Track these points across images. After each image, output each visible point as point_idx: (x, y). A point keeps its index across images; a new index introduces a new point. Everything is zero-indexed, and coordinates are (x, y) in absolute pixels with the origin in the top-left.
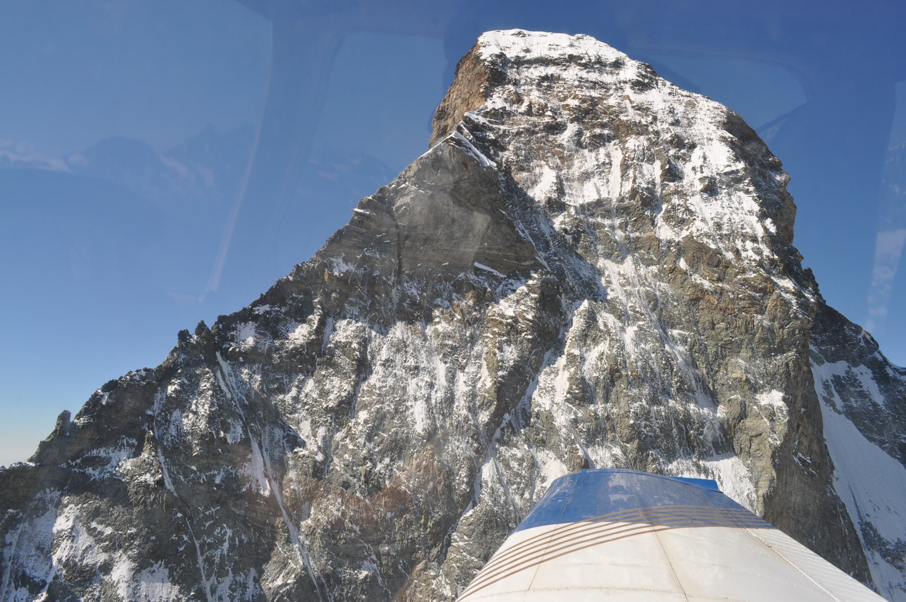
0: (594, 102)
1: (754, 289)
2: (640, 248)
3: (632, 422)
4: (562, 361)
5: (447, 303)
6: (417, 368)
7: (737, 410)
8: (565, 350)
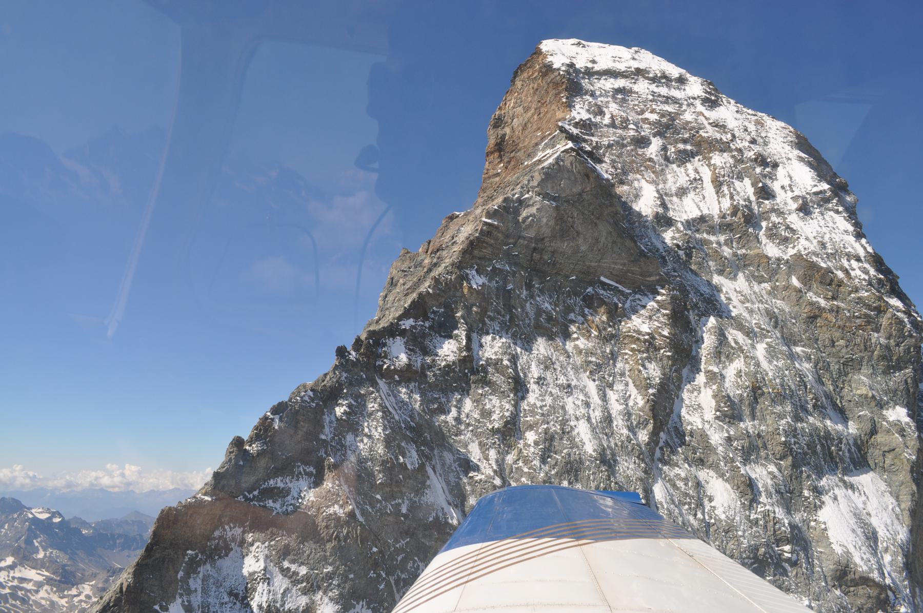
0: (673, 117)
1: (869, 307)
2: (749, 265)
3: (783, 439)
4: (701, 378)
5: (580, 318)
6: (569, 386)
7: (868, 427)
8: (702, 367)
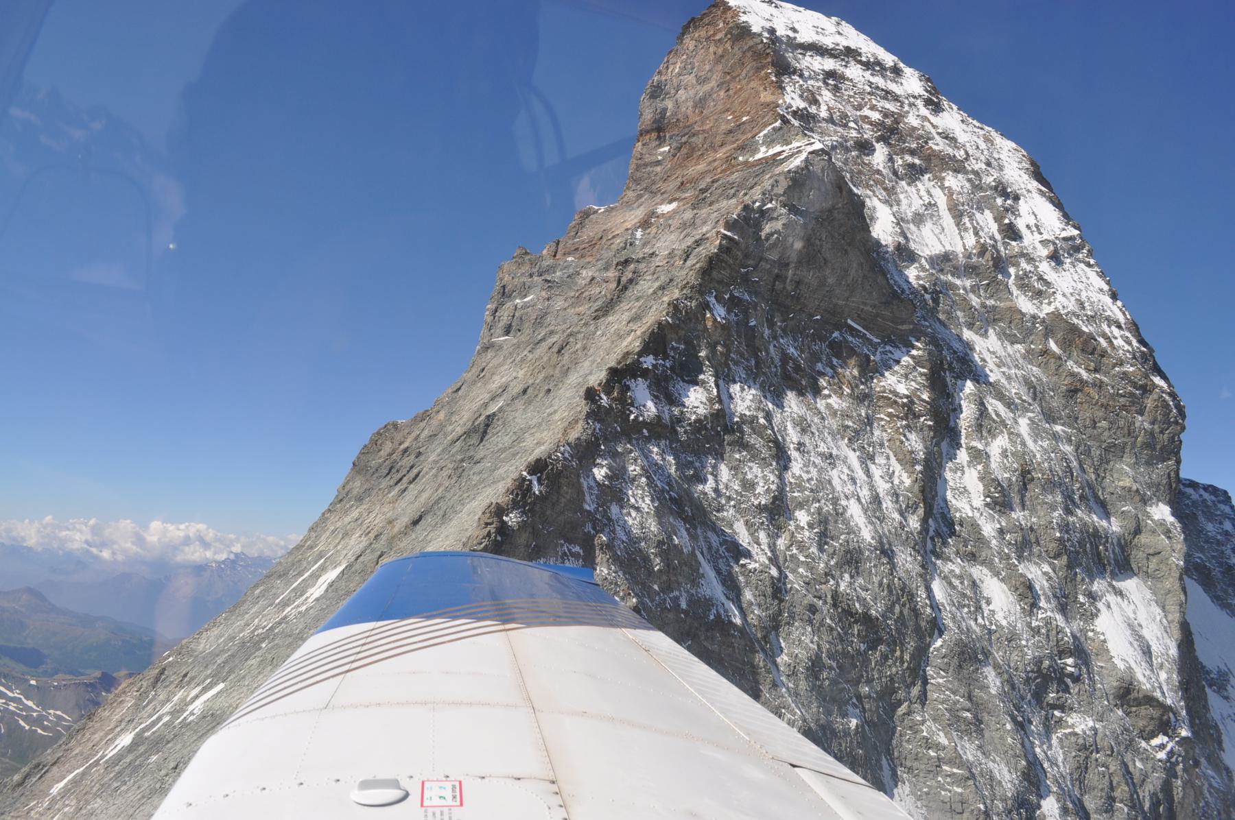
1: (1135, 385)
2: (1000, 320)
3: (1058, 535)
4: (963, 456)
5: (828, 370)
6: (831, 455)
7: (1132, 525)
8: (963, 441)
